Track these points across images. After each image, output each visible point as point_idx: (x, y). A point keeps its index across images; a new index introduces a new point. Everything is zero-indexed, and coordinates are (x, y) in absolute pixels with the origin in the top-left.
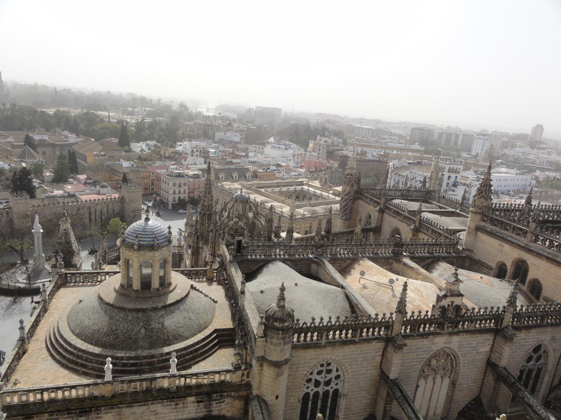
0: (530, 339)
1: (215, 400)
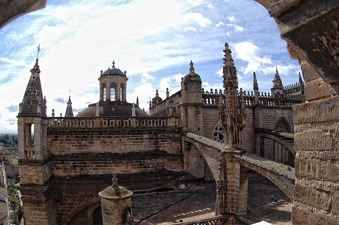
1: (160, 139)
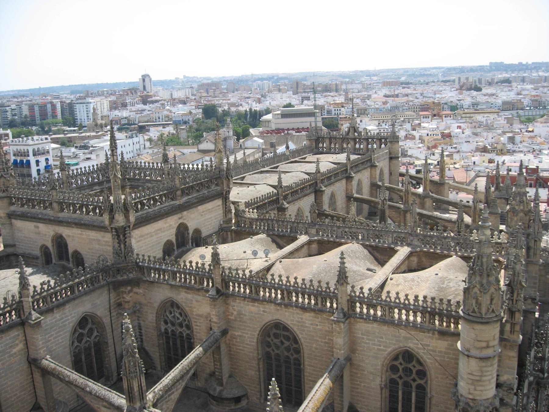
0: (67, 316)
